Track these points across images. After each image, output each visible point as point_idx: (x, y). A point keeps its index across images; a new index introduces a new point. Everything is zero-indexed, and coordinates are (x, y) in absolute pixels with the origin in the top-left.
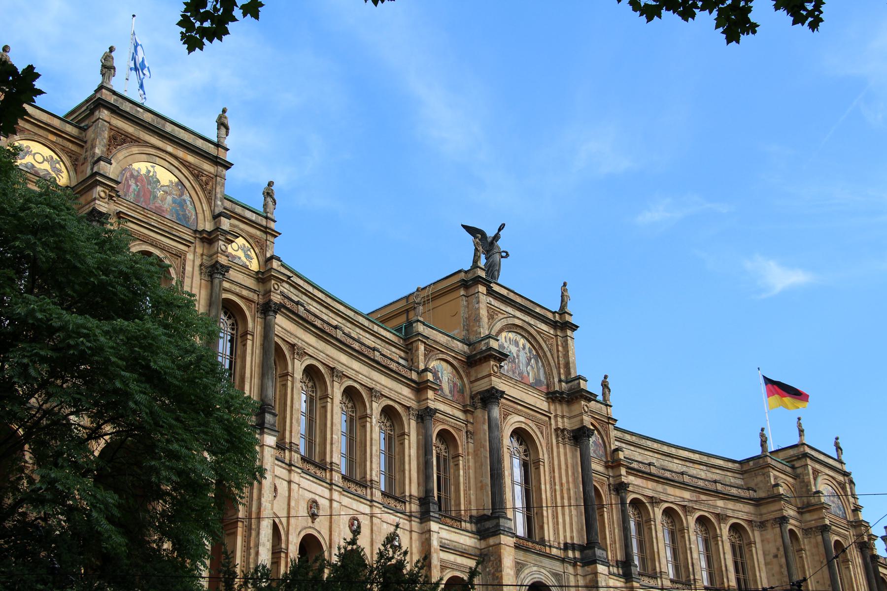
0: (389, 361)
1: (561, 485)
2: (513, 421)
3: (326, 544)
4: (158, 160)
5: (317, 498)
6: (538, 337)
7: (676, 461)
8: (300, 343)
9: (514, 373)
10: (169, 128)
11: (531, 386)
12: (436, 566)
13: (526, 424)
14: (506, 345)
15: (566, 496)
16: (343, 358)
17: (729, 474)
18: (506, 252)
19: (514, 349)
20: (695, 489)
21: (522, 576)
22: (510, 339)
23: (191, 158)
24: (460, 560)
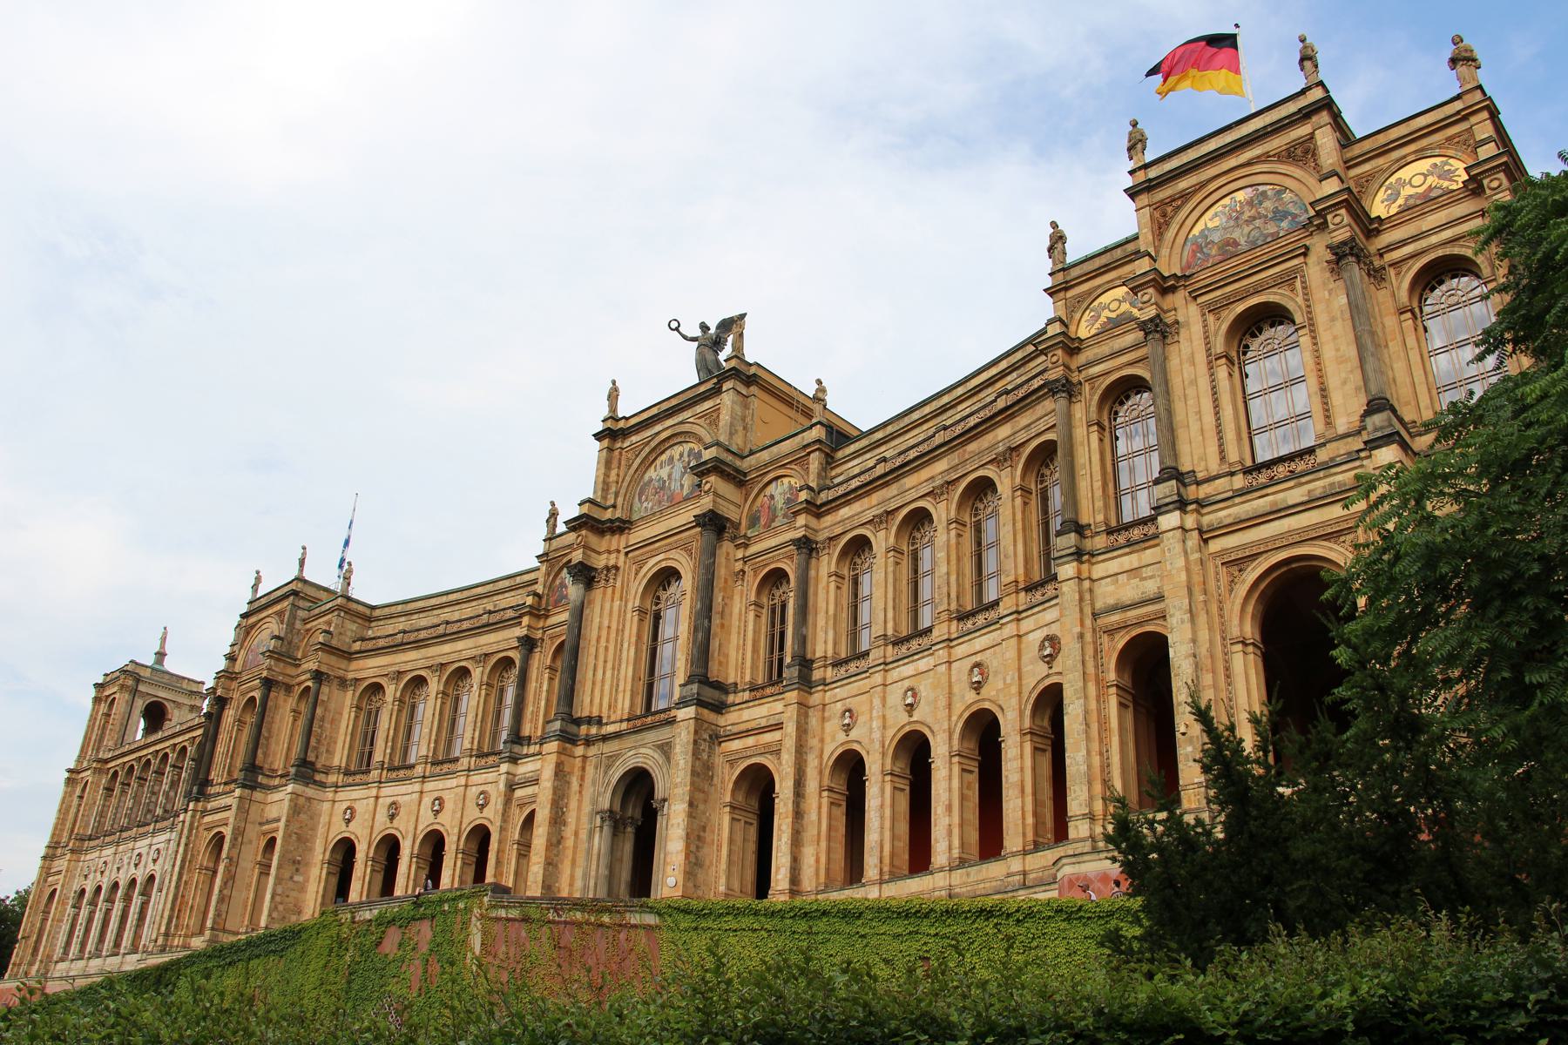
4: (263, 627)
5: (399, 798)
10: (272, 597)
16: (447, 648)
20: (949, 446)
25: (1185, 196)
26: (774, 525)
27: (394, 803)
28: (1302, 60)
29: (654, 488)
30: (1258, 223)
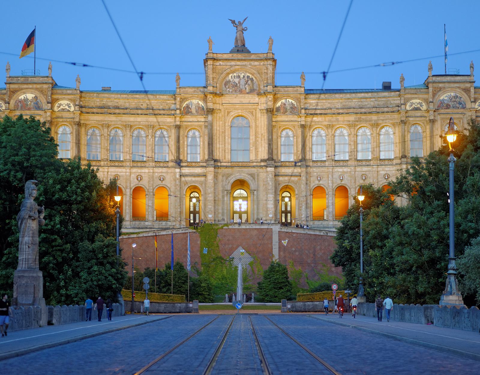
1: (262, 134)
2: (232, 114)
5: (119, 173)
7: (354, 100)
8: (107, 123)
9: (236, 91)
11: (248, 93)
12: (177, 185)
15: (263, 139)
17: (390, 99)
19: (237, 80)
21: (230, 179)
23: (38, 86)
24: (194, 179)
25: (440, 89)
27: (116, 174)
28: (471, 67)
29: (232, 84)
30: (455, 103)
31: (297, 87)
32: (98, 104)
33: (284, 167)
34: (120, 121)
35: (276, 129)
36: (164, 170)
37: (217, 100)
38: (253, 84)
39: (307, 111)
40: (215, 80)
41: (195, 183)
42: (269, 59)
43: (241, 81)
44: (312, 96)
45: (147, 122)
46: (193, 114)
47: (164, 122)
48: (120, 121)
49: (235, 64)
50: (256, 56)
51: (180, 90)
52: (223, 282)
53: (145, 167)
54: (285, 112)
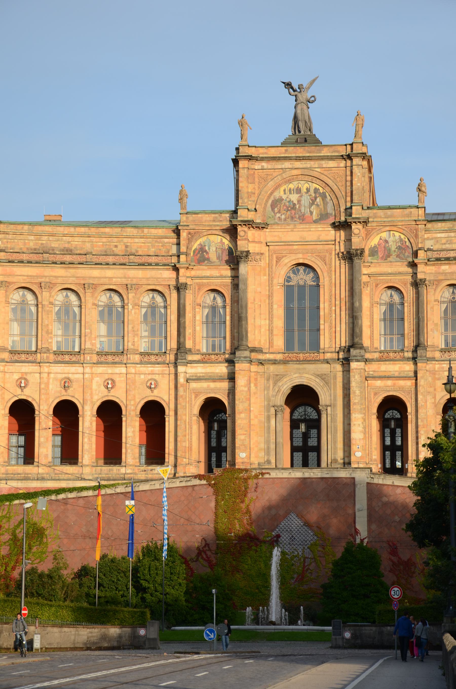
0: (147, 257)
3: (80, 402)
5: (70, 376)
6: (322, 177)
8: (47, 280)
9: (292, 218)
11: (315, 222)
12: (182, 396)
13: (303, 259)
14: (284, 197)
16: (96, 273)
18: (314, 97)
19: (294, 198)
21: (280, 384)
22: (290, 189)
26: (389, 259)
27: (65, 378)
31: (410, 207)
32: (32, 245)
33: (386, 361)
34: (73, 277)
35: (369, 288)
36: (158, 369)
37: (256, 235)
38: (325, 204)
39: (429, 253)
40: (253, 198)
41: (215, 393)
42: (357, 155)
43: (303, 199)
44: (440, 225)
45: (125, 278)
46: (212, 262)
47: (157, 278)
48: (73, 277)
49: (290, 166)
50: (332, 149)
51: (187, 218)
52: (259, 582)
53: (120, 363)
54: (387, 255)
